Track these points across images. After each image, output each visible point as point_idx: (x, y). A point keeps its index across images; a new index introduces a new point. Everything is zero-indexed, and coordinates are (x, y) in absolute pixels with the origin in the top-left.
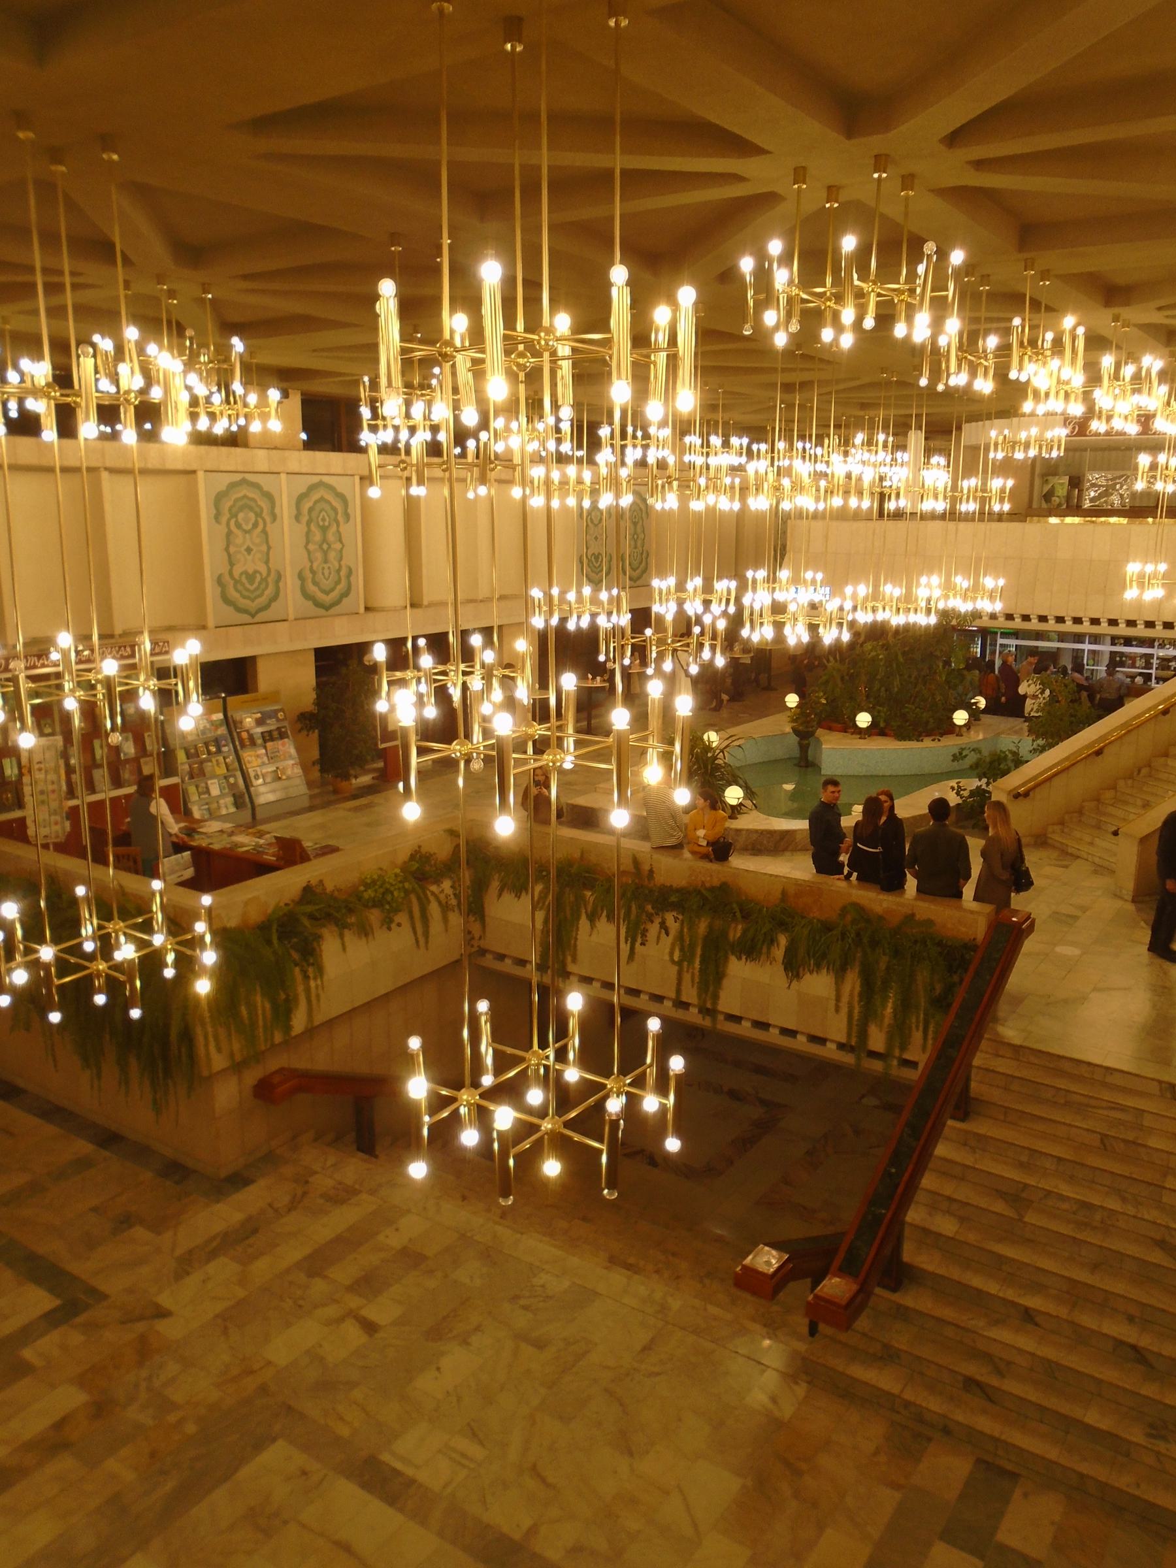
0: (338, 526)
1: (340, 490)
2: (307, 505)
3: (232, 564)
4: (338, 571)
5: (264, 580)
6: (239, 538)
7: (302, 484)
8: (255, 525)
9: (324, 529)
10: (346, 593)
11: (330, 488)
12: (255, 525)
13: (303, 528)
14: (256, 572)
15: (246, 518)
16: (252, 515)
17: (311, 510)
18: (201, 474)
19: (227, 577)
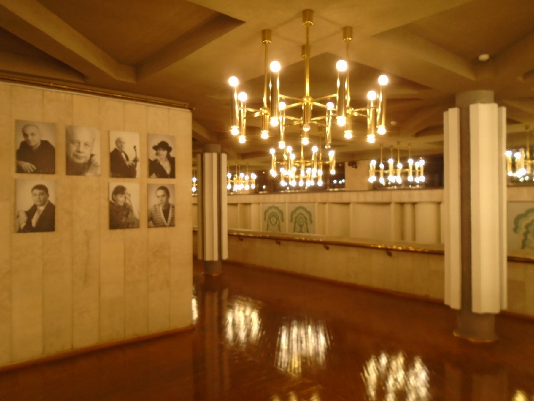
0: (307, 224)
1: (308, 210)
9: (301, 226)
11: (305, 209)
12: (276, 223)
13: (293, 225)
16: (275, 219)
17: (296, 218)
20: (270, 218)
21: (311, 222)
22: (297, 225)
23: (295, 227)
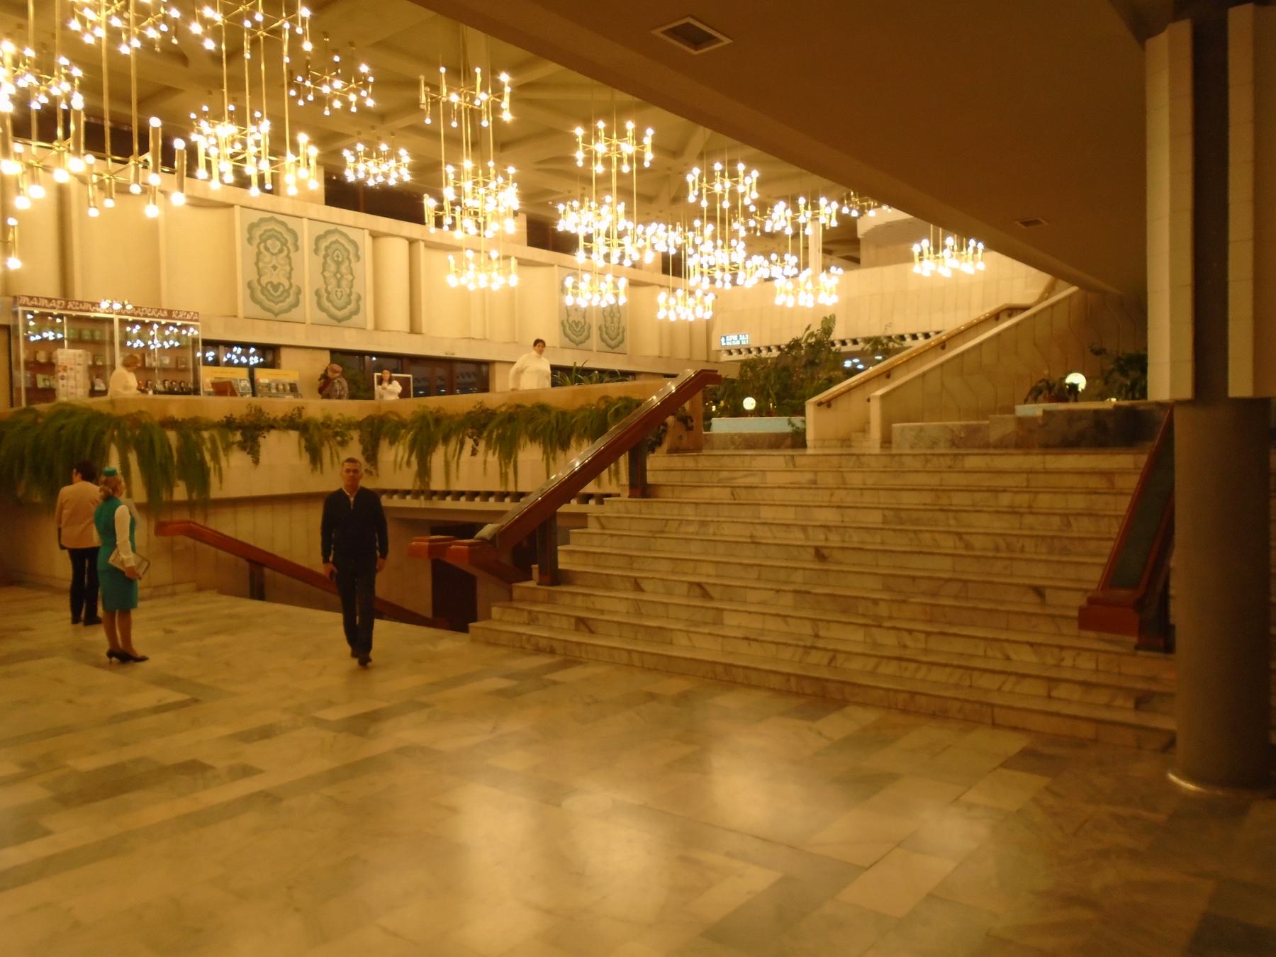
2: (323, 244)
3: (260, 275)
5: (287, 291)
6: (267, 257)
7: (322, 229)
8: (281, 251)
9: (338, 264)
10: (356, 312)
12: (281, 251)
14: (279, 284)
15: (274, 245)
17: (327, 248)
18: (237, 208)
20: (263, 240)
21: (358, 258)
22: (329, 260)
23: (324, 264)
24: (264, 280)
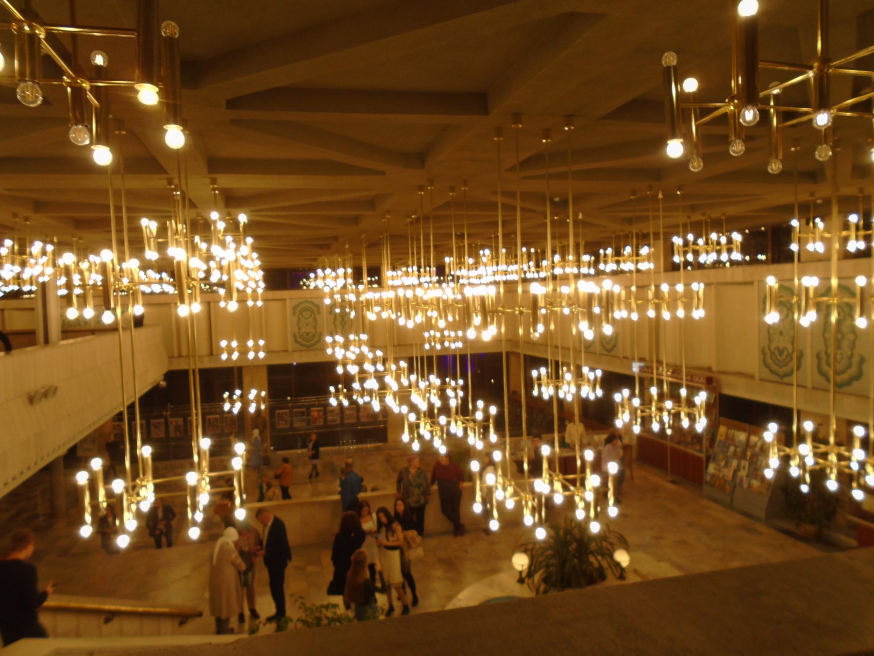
3: (770, 341)
4: (851, 357)
5: (790, 356)
14: (785, 348)
19: (767, 350)
24: (773, 346)
